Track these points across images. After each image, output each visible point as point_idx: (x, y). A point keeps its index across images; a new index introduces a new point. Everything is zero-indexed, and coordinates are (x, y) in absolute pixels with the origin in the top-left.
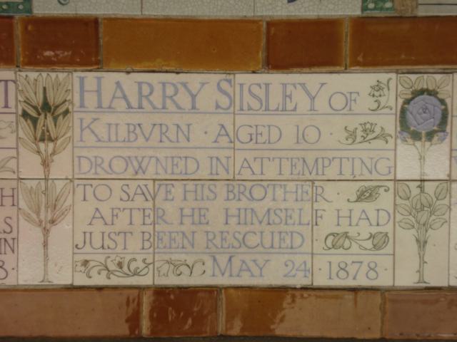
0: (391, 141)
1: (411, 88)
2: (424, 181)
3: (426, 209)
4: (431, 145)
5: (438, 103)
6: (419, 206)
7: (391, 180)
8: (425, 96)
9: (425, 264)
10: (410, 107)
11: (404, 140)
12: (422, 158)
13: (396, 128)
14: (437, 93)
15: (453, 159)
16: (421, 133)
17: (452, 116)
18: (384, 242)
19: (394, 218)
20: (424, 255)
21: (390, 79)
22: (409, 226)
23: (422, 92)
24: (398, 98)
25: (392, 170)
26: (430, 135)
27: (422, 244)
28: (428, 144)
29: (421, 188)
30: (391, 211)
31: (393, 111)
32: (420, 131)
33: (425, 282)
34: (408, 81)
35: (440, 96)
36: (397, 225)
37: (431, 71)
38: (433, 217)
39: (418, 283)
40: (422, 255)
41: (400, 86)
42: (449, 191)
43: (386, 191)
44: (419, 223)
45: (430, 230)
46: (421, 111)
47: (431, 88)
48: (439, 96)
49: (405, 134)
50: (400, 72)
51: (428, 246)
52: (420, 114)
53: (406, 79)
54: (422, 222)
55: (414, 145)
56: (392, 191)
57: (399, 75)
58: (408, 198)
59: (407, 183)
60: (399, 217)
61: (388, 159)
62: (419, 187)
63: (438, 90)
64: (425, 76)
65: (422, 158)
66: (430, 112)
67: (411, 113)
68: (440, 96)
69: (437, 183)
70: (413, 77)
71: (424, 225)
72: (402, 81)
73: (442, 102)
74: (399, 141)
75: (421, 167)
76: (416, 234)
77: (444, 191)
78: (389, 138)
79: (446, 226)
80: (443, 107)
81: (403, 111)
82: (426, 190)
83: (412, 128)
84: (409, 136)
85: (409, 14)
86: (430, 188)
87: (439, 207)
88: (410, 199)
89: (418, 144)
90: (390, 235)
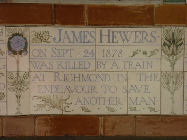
0: (4, 55)
1: (12, 33)
2: (19, 71)
3: (20, 83)
4: (21, 56)
5: (23, 39)
6: (17, 82)
7: (5, 71)
8: (18, 36)
9: (20, 106)
10: (11, 41)
11: (10, 54)
12: (18, 62)
13: (6, 49)
14: (23, 35)
15: (30, 62)
16: (16, 52)
17: (29, 45)
18: (3, 97)
19: (7, 87)
20: (19, 102)
21: (3, 29)
22: (13, 90)
23: (16, 34)
24: (7, 37)
25: (5, 67)
26: (21, 53)
27: (18, 97)
28: (20, 56)
29: (18, 74)
30: (5, 84)
31: (5, 42)
32: (16, 50)
33: (20, 113)
34: (11, 30)
35: (24, 36)
36: (8, 89)
37: (20, 26)
38: (23, 86)
39: (17, 113)
40: (18, 102)
41: (7, 32)
42: (29, 75)
43: (3, 75)
44: (17, 89)
45: (22, 92)
46: (16, 43)
47: (20, 33)
48: (23, 36)
50: (7, 26)
51: (21, 98)
52: (16, 44)
53: (9, 29)
54: (18, 88)
55: (14, 56)
56: (5, 75)
57: (6, 27)
58: (13, 79)
59: (12, 72)
60: (9, 86)
61: (3, 62)
62: (17, 74)
63: (23, 34)
64: (18, 28)
65: (18, 62)
67: (12, 43)
68: (24, 36)
69: (24, 72)
70: (13, 28)
71: (19, 89)
72: (8, 30)
73: (25, 39)
74: (7, 55)
75: (18, 66)
76: (16, 93)
77: (27, 76)
78: (3, 53)
79: (28, 90)
80: (25, 41)
81: (9, 43)
82: (20, 75)
84: (12, 53)
85: (9, 2)
86: (21, 74)
87: (26, 82)
88: (13, 79)
89: (16, 56)
90: (5, 94)
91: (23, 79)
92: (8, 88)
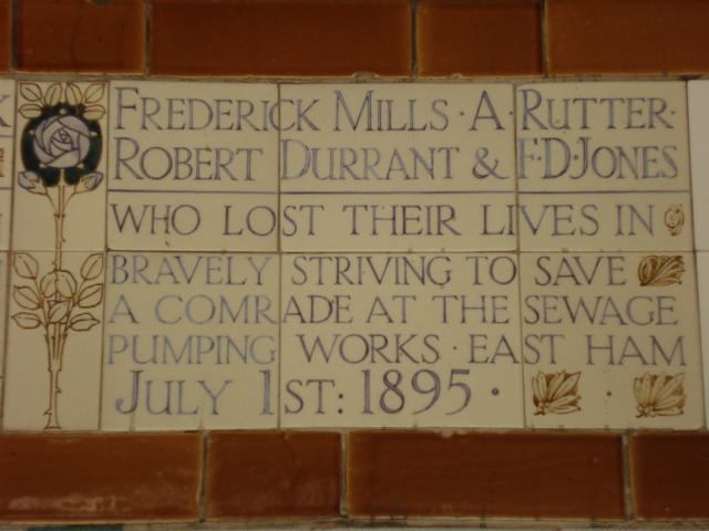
4: (75, 192)
5: (84, 129)
26: (73, 176)
28: (70, 189)
41: (20, 97)
47: (72, 102)
49: (32, 175)
55: (46, 194)
65: (59, 216)
66: (72, 143)
68: (88, 116)
72: (25, 91)
73: (94, 125)
80: (94, 134)
83: (42, 166)
89: (53, 191)
91: (80, 280)
92: (11, 314)
